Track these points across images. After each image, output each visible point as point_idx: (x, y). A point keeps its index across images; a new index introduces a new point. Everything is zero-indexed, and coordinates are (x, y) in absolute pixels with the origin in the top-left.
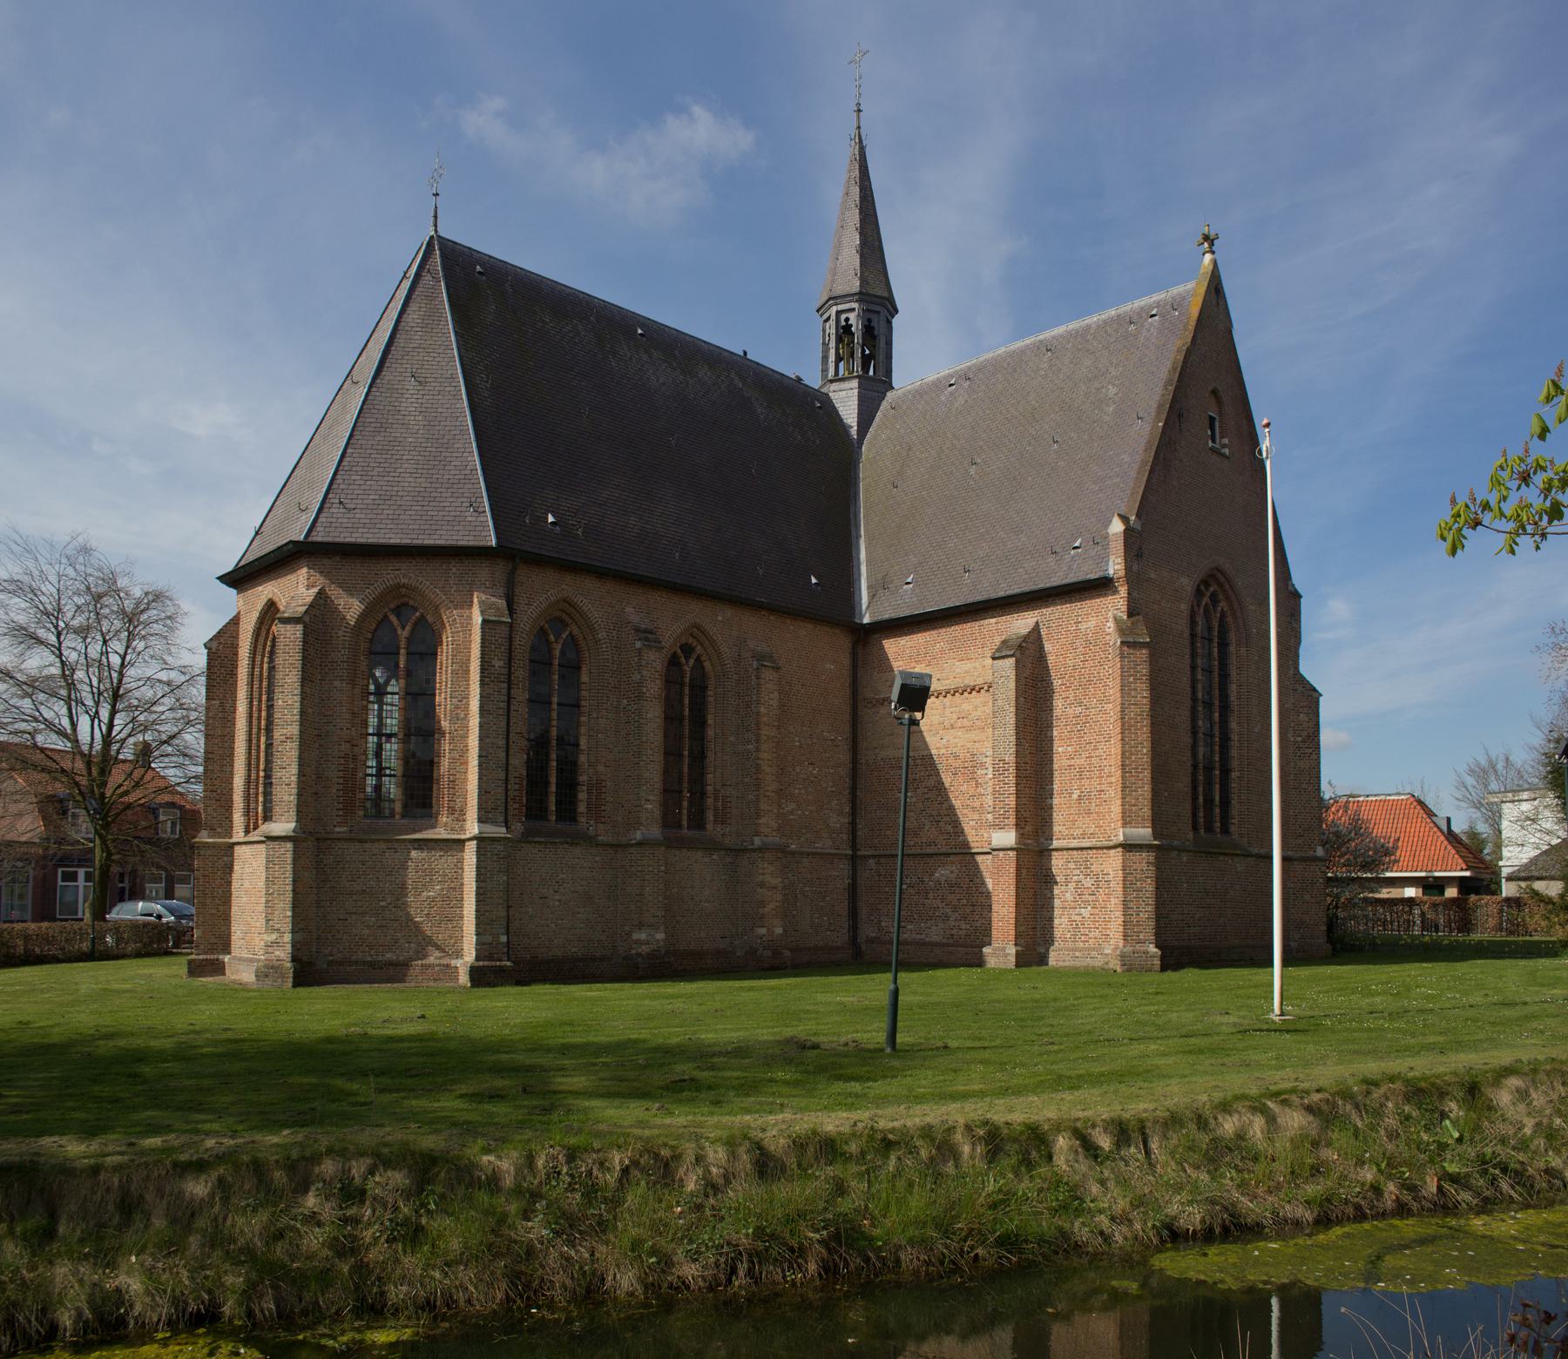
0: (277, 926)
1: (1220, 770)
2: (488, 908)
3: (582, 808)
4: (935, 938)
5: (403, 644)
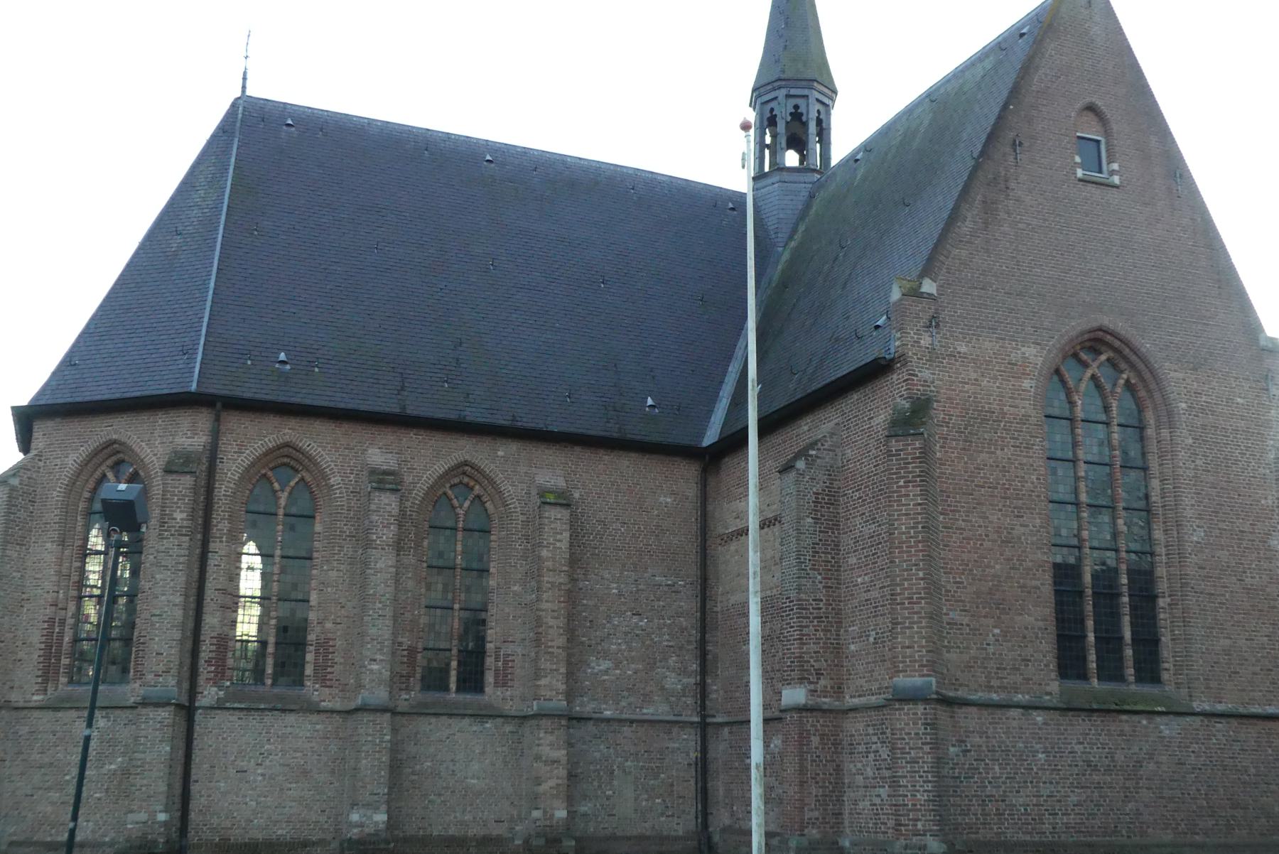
1: (1130, 596)
2: (145, 782)
3: (309, 670)
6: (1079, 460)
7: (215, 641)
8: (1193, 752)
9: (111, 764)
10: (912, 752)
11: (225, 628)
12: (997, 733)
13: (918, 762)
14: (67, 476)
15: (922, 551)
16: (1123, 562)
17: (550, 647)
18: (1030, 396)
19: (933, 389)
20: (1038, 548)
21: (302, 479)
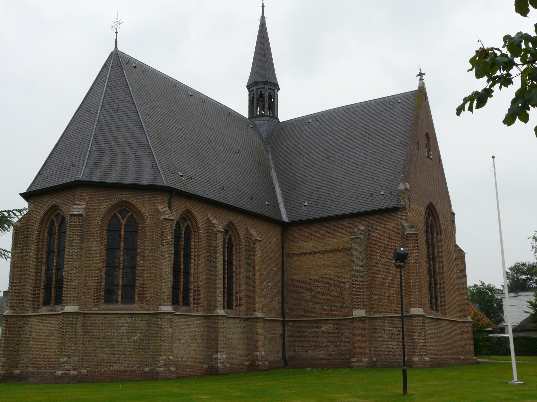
0: (67, 354)
3: (191, 300)
4: (322, 356)
5: (123, 227)
9: (135, 337)
14: (102, 214)
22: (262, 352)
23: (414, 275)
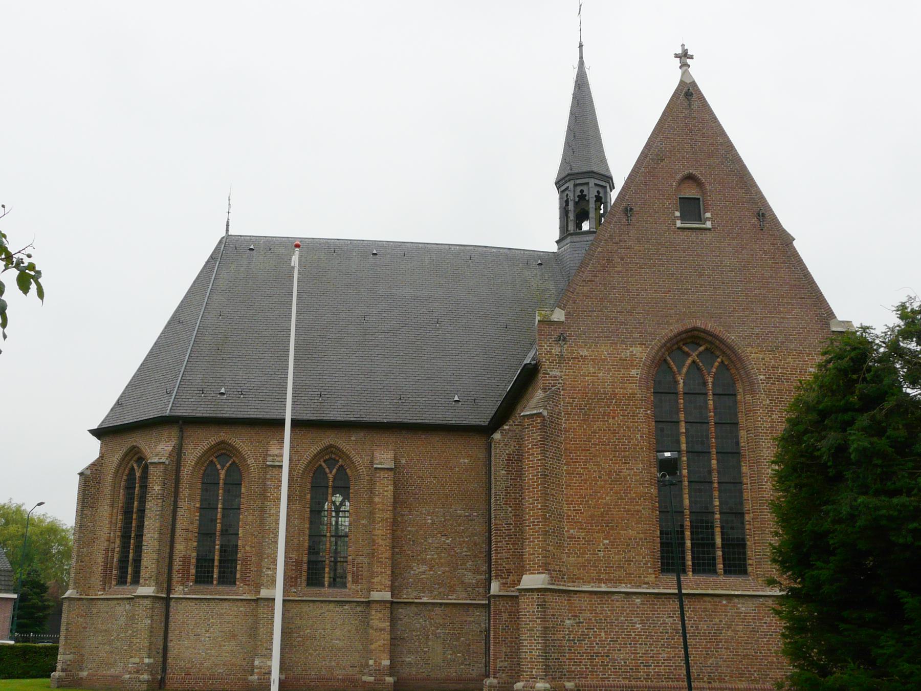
1: (721, 513)
2: (138, 641)
3: (238, 576)
6: (681, 421)
7: (181, 559)
8: (765, 623)
10: (531, 623)
11: (188, 552)
12: (604, 610)
13: (534, 631)
15: (540, 491)
16: (715, 490)
17: (381, 558)
18: (637, 380)
19: (561, 381)
20: (640, 484)
21: (234, 462)
22: (382, 659)
23: (532, 504)
